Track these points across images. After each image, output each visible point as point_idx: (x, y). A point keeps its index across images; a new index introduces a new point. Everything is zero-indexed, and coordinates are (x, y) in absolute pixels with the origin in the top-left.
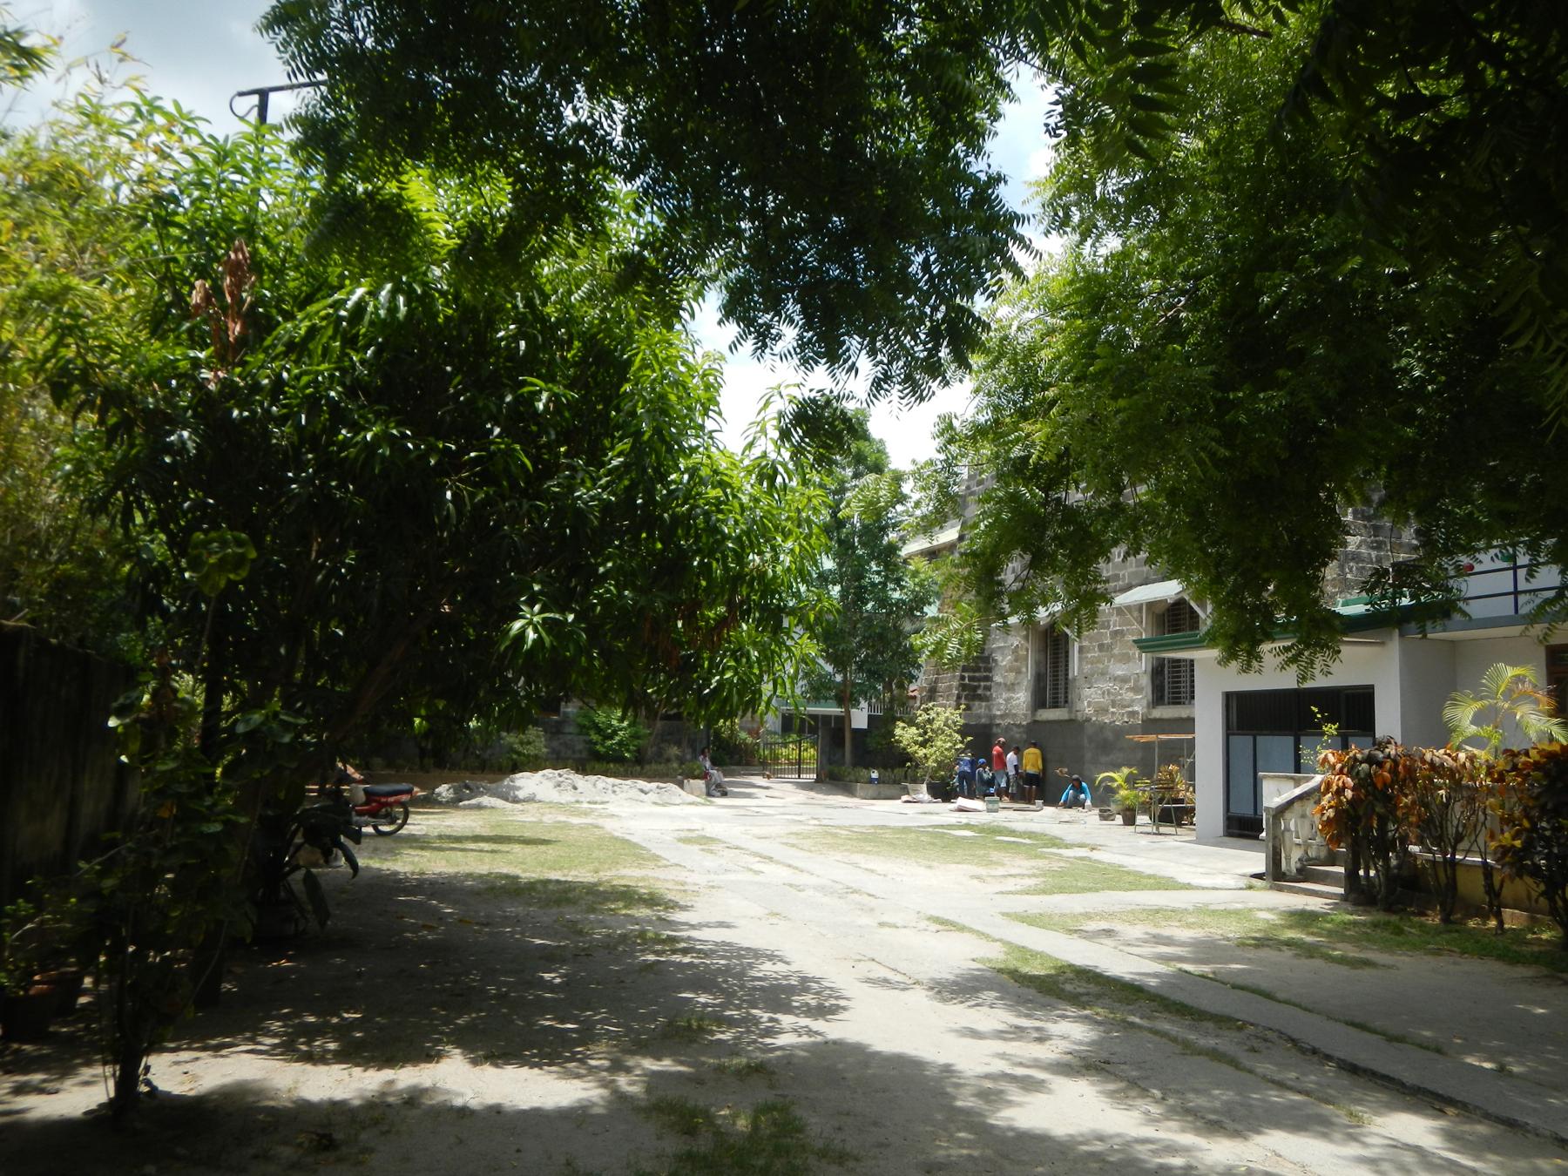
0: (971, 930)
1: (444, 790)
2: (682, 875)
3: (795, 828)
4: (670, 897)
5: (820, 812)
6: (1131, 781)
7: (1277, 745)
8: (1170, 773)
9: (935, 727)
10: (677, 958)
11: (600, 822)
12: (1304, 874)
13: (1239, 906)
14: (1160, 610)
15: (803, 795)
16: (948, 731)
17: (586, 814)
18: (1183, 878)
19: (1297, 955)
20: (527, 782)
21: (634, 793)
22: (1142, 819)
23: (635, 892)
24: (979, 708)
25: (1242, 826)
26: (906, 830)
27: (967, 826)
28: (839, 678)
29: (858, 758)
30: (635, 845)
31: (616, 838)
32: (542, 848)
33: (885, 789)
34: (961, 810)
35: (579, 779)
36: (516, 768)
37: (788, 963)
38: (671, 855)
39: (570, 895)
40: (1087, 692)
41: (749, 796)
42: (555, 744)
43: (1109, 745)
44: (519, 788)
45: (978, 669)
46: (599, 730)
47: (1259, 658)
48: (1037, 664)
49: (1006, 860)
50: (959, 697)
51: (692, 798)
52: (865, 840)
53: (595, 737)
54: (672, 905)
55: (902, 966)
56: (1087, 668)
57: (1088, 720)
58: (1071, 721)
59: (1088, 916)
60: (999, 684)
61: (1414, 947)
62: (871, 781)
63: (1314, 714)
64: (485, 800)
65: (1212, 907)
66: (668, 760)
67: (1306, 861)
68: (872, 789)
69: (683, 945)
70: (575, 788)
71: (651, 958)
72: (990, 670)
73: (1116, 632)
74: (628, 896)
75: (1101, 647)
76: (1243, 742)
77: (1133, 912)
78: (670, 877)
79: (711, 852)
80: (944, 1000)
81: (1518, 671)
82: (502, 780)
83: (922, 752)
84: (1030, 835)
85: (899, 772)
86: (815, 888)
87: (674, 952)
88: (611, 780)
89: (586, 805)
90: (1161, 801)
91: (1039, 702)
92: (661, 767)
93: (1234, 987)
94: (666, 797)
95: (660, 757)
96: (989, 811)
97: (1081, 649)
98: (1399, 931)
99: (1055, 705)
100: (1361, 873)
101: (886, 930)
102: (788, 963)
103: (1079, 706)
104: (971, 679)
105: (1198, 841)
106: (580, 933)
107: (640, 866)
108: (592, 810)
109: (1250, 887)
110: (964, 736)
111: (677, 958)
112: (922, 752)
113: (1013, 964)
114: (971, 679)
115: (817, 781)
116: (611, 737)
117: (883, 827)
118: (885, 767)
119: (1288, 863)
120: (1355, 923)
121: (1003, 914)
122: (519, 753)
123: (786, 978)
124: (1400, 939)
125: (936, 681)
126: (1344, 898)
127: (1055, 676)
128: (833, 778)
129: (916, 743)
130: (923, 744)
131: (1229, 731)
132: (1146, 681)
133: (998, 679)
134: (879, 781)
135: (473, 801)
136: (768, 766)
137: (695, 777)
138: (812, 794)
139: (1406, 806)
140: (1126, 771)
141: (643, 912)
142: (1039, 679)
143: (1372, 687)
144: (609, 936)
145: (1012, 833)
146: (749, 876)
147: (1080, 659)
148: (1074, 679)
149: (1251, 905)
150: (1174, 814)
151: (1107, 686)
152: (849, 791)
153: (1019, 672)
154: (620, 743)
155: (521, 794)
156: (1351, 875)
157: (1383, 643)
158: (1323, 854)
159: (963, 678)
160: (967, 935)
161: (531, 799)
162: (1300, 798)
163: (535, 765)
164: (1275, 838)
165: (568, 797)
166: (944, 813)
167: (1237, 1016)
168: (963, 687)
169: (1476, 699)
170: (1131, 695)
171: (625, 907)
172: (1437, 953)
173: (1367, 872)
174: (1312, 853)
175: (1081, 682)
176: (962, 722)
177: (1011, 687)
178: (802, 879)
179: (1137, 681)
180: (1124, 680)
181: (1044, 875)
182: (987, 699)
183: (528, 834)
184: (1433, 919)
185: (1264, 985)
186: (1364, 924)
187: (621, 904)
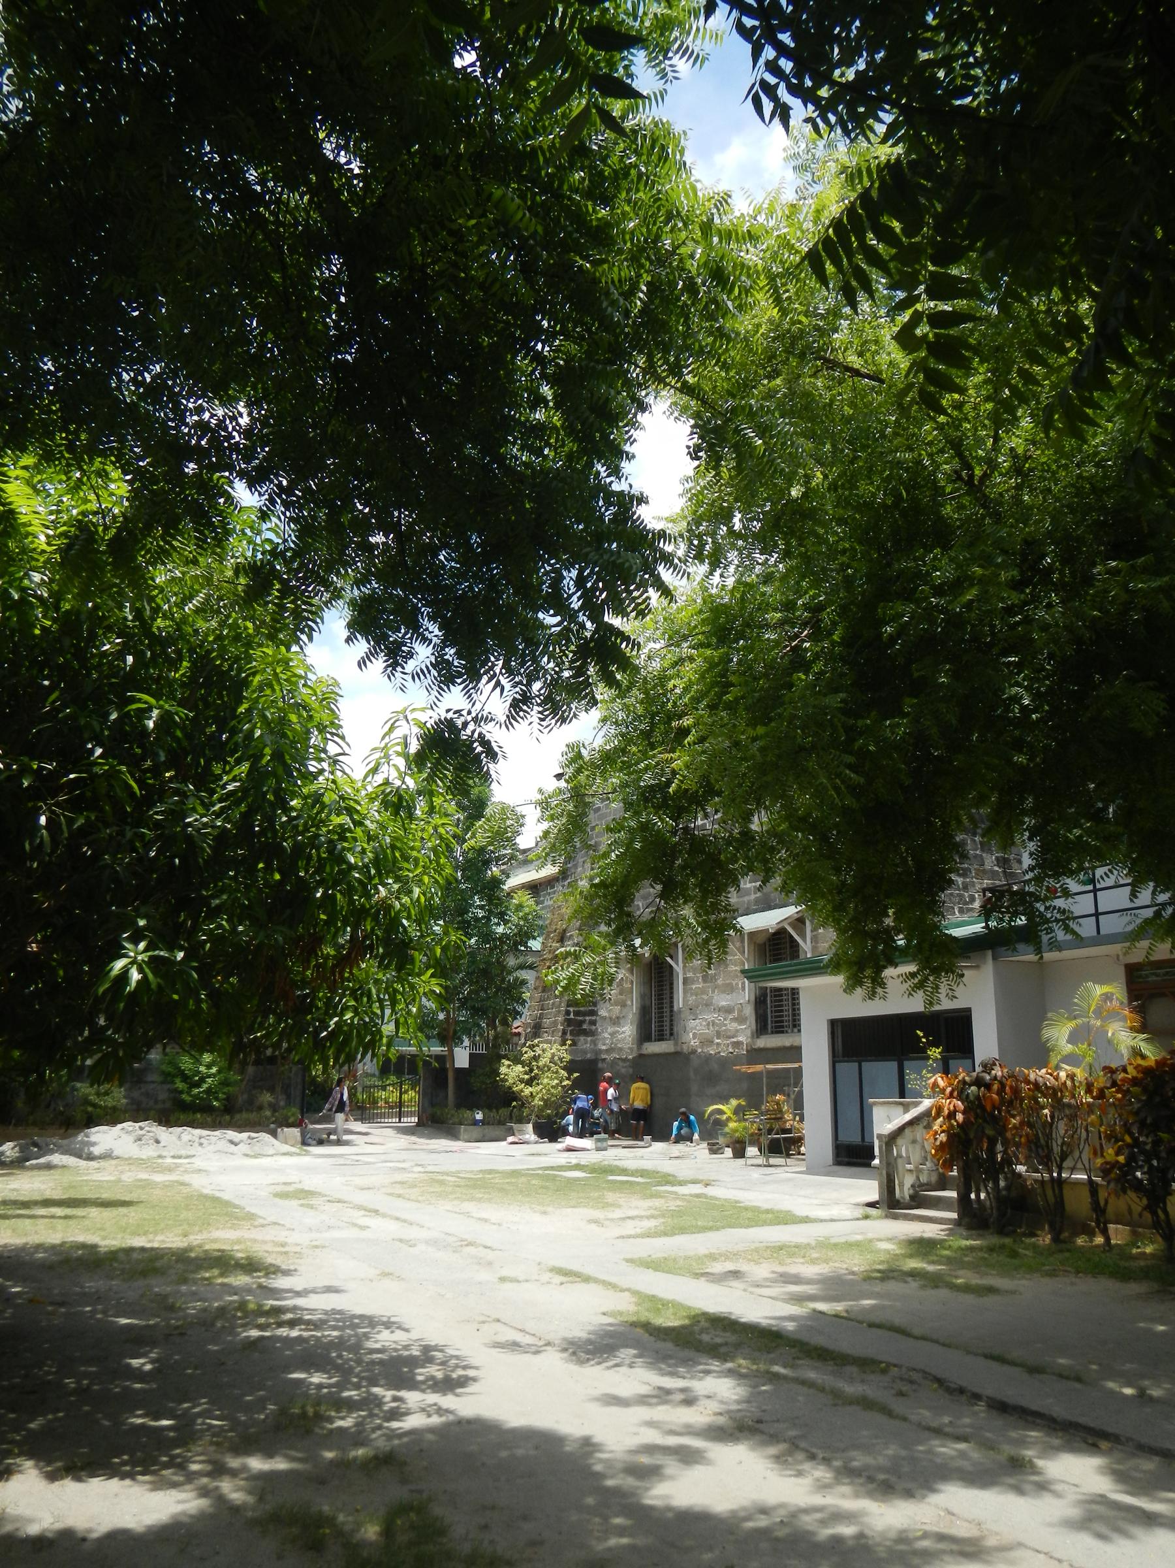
0: (596, 1281)
2: (282, 1235)
3: (399, 1177)
4: (270, 1260)
5: (423, 1157)
6: (738, 1111)
7: (883, 1071)
8: (778, 1103)
9: (540, 1064)
10: (283, 1332)
11: (186, 1178)
12: (918, 1201)
13: (859, 1237)
14: (761, 939)
15: (405, 1140)
16: (554, 1068)
17: (170, 1169)
18: (801, 1212)
19: (923, 1287)
20: (103, 1137)
21: (223, 1145)
22: (752, 1151)
23: (232, 1257)
24: (585, 1043)
25: (852, 1154)
26: (515, 1173)
27: (578, 1167)
28: (441, 1016)
29: (463, 1099)
30: (227, 1204)
31: (206, 1197)
32: (123, 1210)
33: (489, 1130)
34: (570, 1149)
35: (162, 1132)
36: (91, 1121)
37: (407, 1330)
38: (267, 1213)
39: (158, 1264)
40: (692, 1023)
41: (347, 1143)
42: (136, 1094)
43: (715, 1075)
44: (94, 1144)
46: (185, 1078)
47: (882, 985)
48: (642, 997)
49: (621, 1202)
50: (564, 1033)
51: (286, 1148)
52: (474, 1187)
53: (180, 1085)
54: (273, 1270)
55: (530, 1326)
56: (692, 999)
57: (694, 1052)
58: (677, 1053)
59: (712, 1257)
60: (604, 1018)
61: (1031, 1270)
62: (475, 1123)
63: (919, 1038)
64: (56, 1158)
65: (833, 1241)
66: (260, 1108)
67: (918, 1186)
68: (476, 1131)
69: (289, 1316)
70: (158, 1142)
71: (254, 1333)
74: (223, 1262)
76: (848, 1069)
77: (757, 1250)
78: (268, 1238)
79: (311, 1207)
80: (581, 1362)
81: (1106, 989)
82: (76, 1135)
83: (528, 1091)
84: (642, 1173)
85: (504, 1112)
86: (427, 1242)
87: (280, 1325)
88: (198, 1132)
89: (169, 1160)
90: (770, 1131)
91: (645, 1035)
92: (253, 1116)
93: (871, 1325)
94: (257, 1148)
95: (252, 1105)
96: (598, 1149)
97: (685, 981)
98: (1014, 1254)
99: (661, 1038)
100: (973, 1196)
101: (508, 1286)
102: (407, 1330)
104: (577, 1013)
105: (810, 1171)
106: (171, 1308)
107: (234, 1227)
108: (177, 1166)
109: (866, 1217)
110: (570, 1072)
111: (283, 1332)
112: (528, 1091)
113: (645, 1316)
114: (577, 1013)
115: (418, 1124)
116: (198, 1085)
117: (490, 1172)
118: (490, 1108)
119: (902, 1190)
120: (971, 1249)
121: (627, 1261)
122: (95, 1106)
123: (406, 1347)
124: (1016, 1262)
125: (541, 1017)
126: (958, 1223)
127: (660, 1008)
128: (436, 1120)
129: (522, 1081)
130: (529, 1083)
131: (836, 1057)
132: (749, 1011)
133: (603, 1013)
134: (484, 1122)
135: (42, 1160)
136: (364, 1111)
137: (289, 1126)
138: (414, 1138)
139: (1015, 1127)
140: (734, 1102)
141: (240, 1280)
142: (644, 1012)
143: (969, 1010)
144: (205, 1310)
145: (624, 1171)
146: (354, 1233)
147: (685, 991)
148: (680, 1011)
149: (870, 1236)
150: (782, 1144)
151: (711, 1017)
152: (453, 1135)
153: (624, 1005)
154: (208, 1091)
155: (96, 1151)
156: (964, 1199)
157: (977, 967)
158: (934, 1178)
159: (568, 1013)
160: (592, 1285)
161: (107, 1156)
162: (911, 1123)
163: (112, 1117)
164: (888, 1164)
165: (149, 1151)
166: (552, 1154)
167: (880, 1358)
168: (569, 1022)
169: (1070, 1019)
170: (735, 1025)
171: (222, 1275)
172: (1052, 1274)
173: (978, 1196)
174: (924, 1179)
175: (686, 1014)
176: (568, 1057)
177: (616, 1021)
178: (413, 1233)
179: (740, 1011)
180: (728, 1010)
181: (663, 1216)
182: (592, 1033)
183: (105, 1195)
184: (1045, 1239)
185: (897, 1321)
186: (980, 1249)
187: (216, 1272)
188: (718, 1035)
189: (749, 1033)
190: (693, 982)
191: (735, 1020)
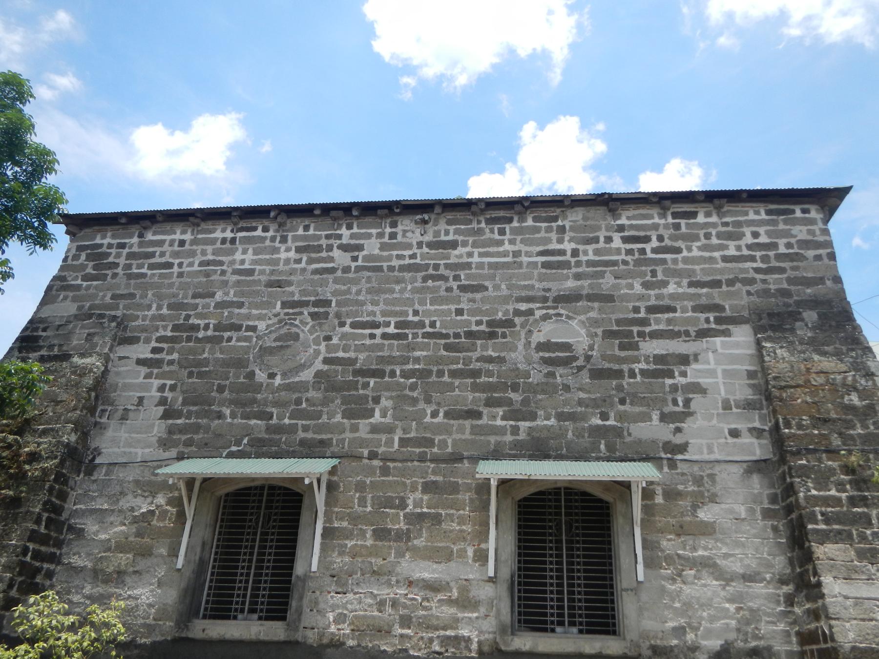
45: (44, 540)
56: (339, 561)
57: (337, 644)
72: (59, 544)
73: (422, 517)
75: (381, 534)
97: (327, 533)
99: (221, 610)
103: (308, 618)
147: (324, 548)
151: (384, 593)
159: (25, 551)
170: (449, 611)
188: (406, 622)
189: (489, 625)
190: (349, 535)
191: (450, 602)
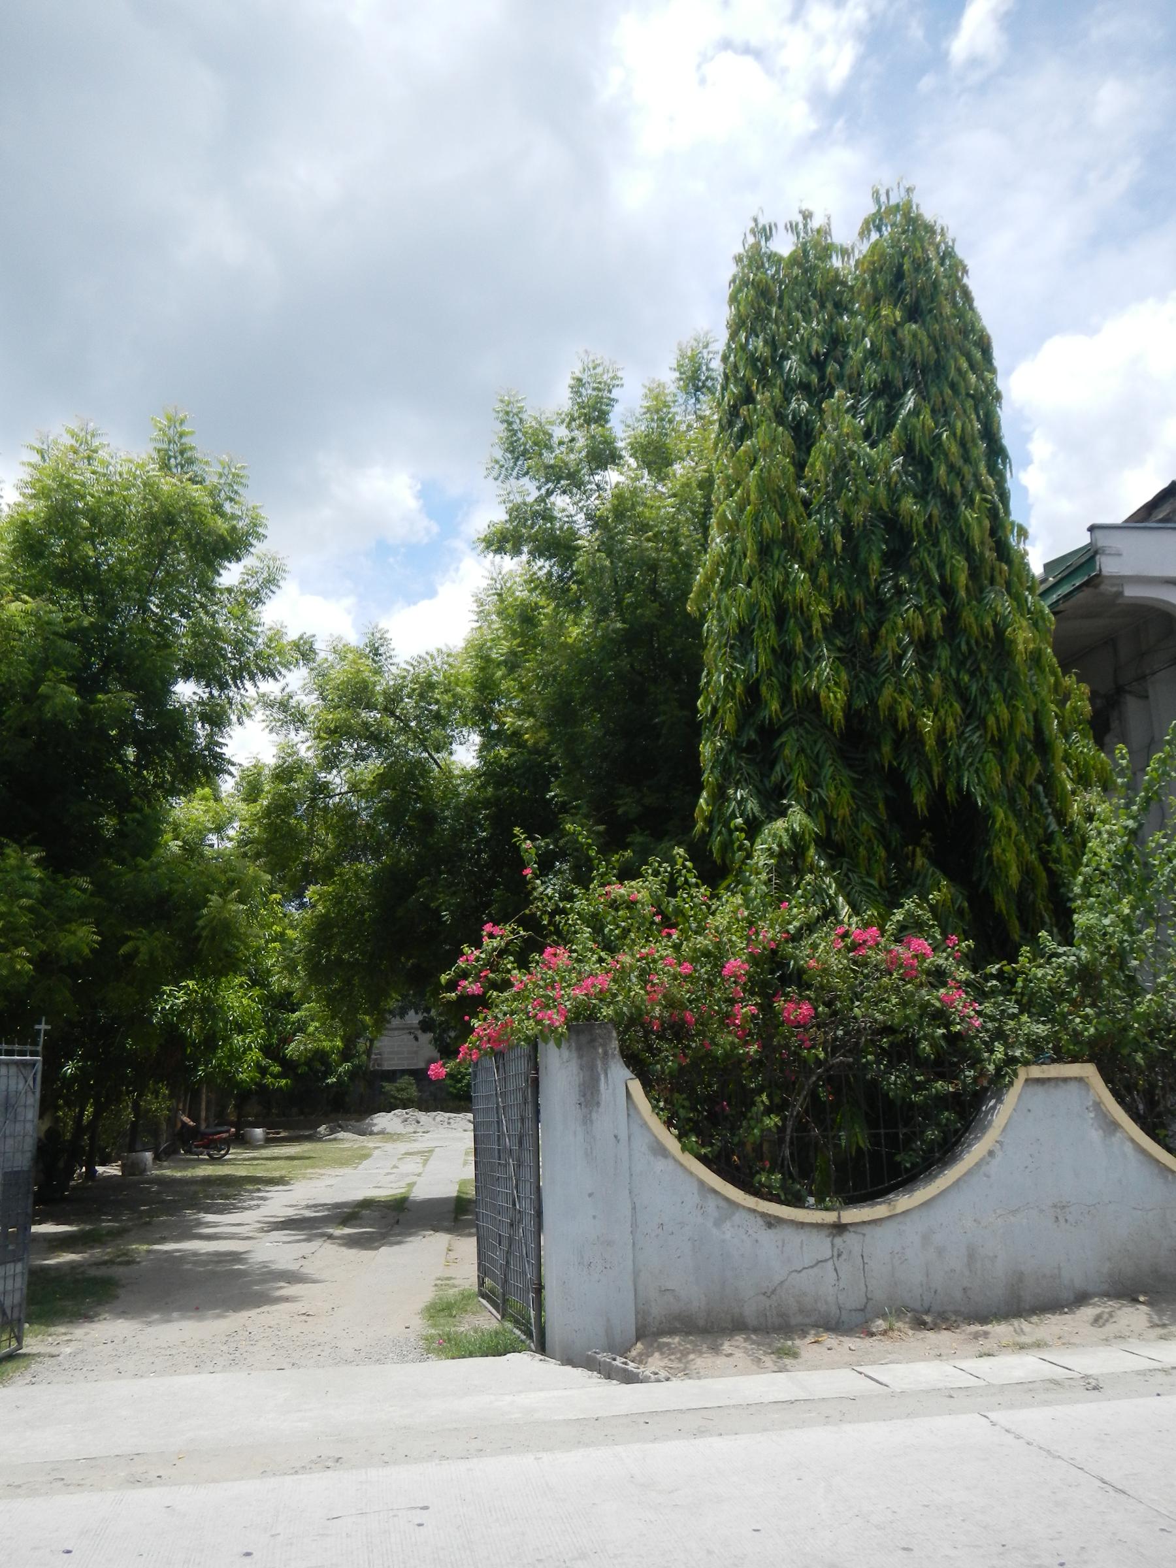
1: (322, 1129)
20: (383, 1121)
35: (423, 1116)
64: (341, 1135)
116: (460, 1081)
122: (396, 1098)
155: (375, 1129)
161: (382, 1132)
